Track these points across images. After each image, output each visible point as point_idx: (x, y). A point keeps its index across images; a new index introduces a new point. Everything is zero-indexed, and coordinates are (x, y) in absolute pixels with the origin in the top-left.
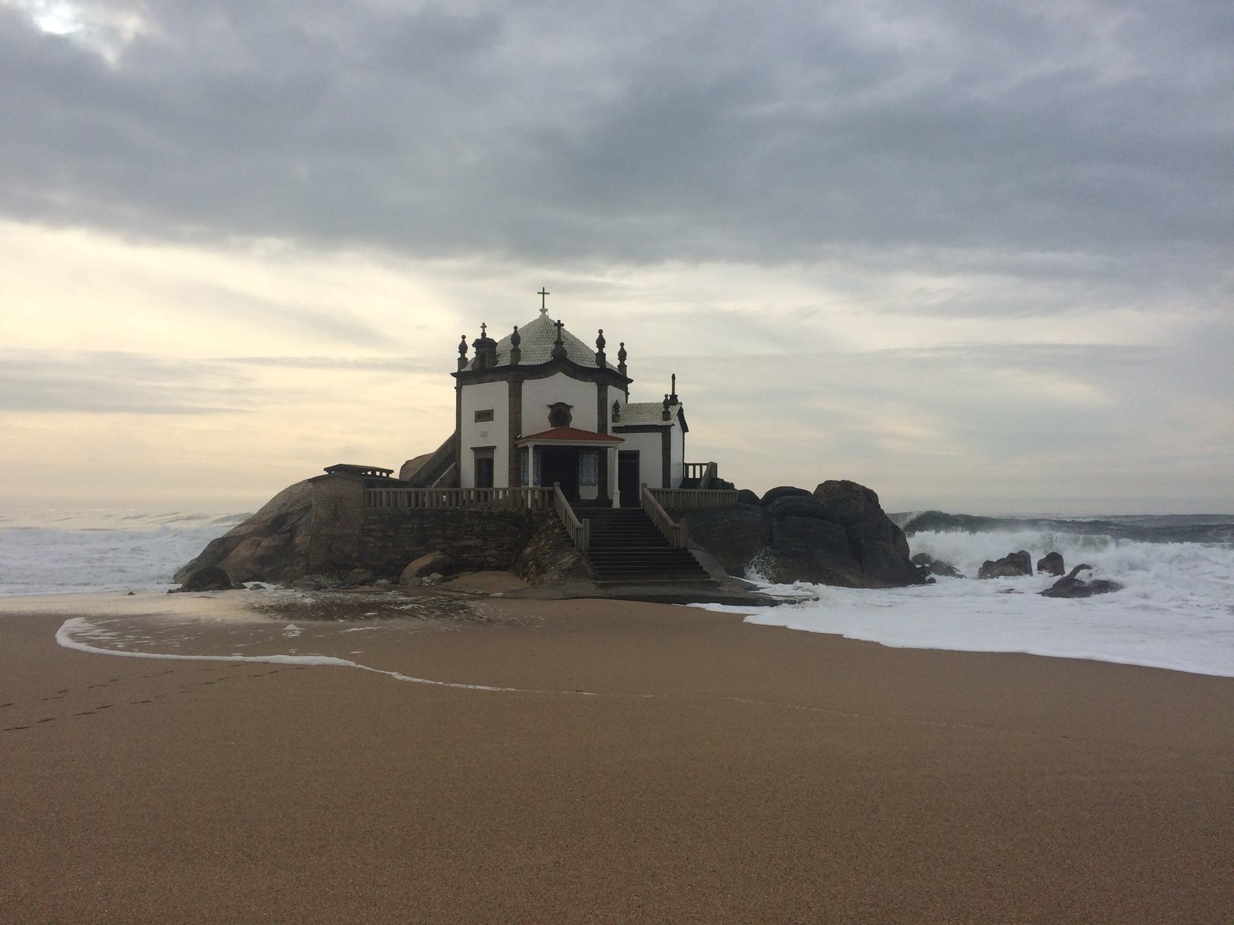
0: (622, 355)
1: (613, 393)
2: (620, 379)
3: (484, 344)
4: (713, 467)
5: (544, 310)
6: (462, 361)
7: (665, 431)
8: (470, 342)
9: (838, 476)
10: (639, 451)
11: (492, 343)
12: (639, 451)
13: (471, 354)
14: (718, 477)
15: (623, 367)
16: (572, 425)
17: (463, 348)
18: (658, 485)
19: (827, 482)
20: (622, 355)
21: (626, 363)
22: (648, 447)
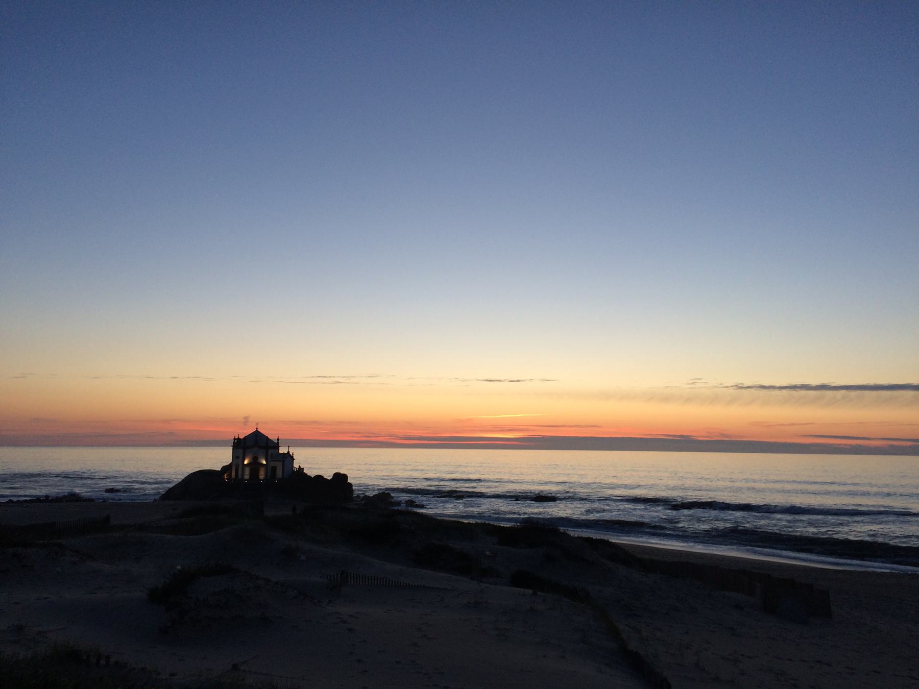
0: (278, 439)
1: (270, 451)
2: (276, 446)
3: (239, 439)
4: (303, 469)
5: (257, 429)
6: (234, 442)
7: (283, 462)
8: (236, 437)
9: (336, 471)
10: (276, 467)
11: (240, 439)
12: (276, 467)
13: (236, 441)
14: (304, 472)
15: (278, 443)
16: (258, 461)
17: (235, 439)
18: (281, 476)
19: (336, 473)
20: (278, 439)
21: (279, 441)
22: (279, 465)
